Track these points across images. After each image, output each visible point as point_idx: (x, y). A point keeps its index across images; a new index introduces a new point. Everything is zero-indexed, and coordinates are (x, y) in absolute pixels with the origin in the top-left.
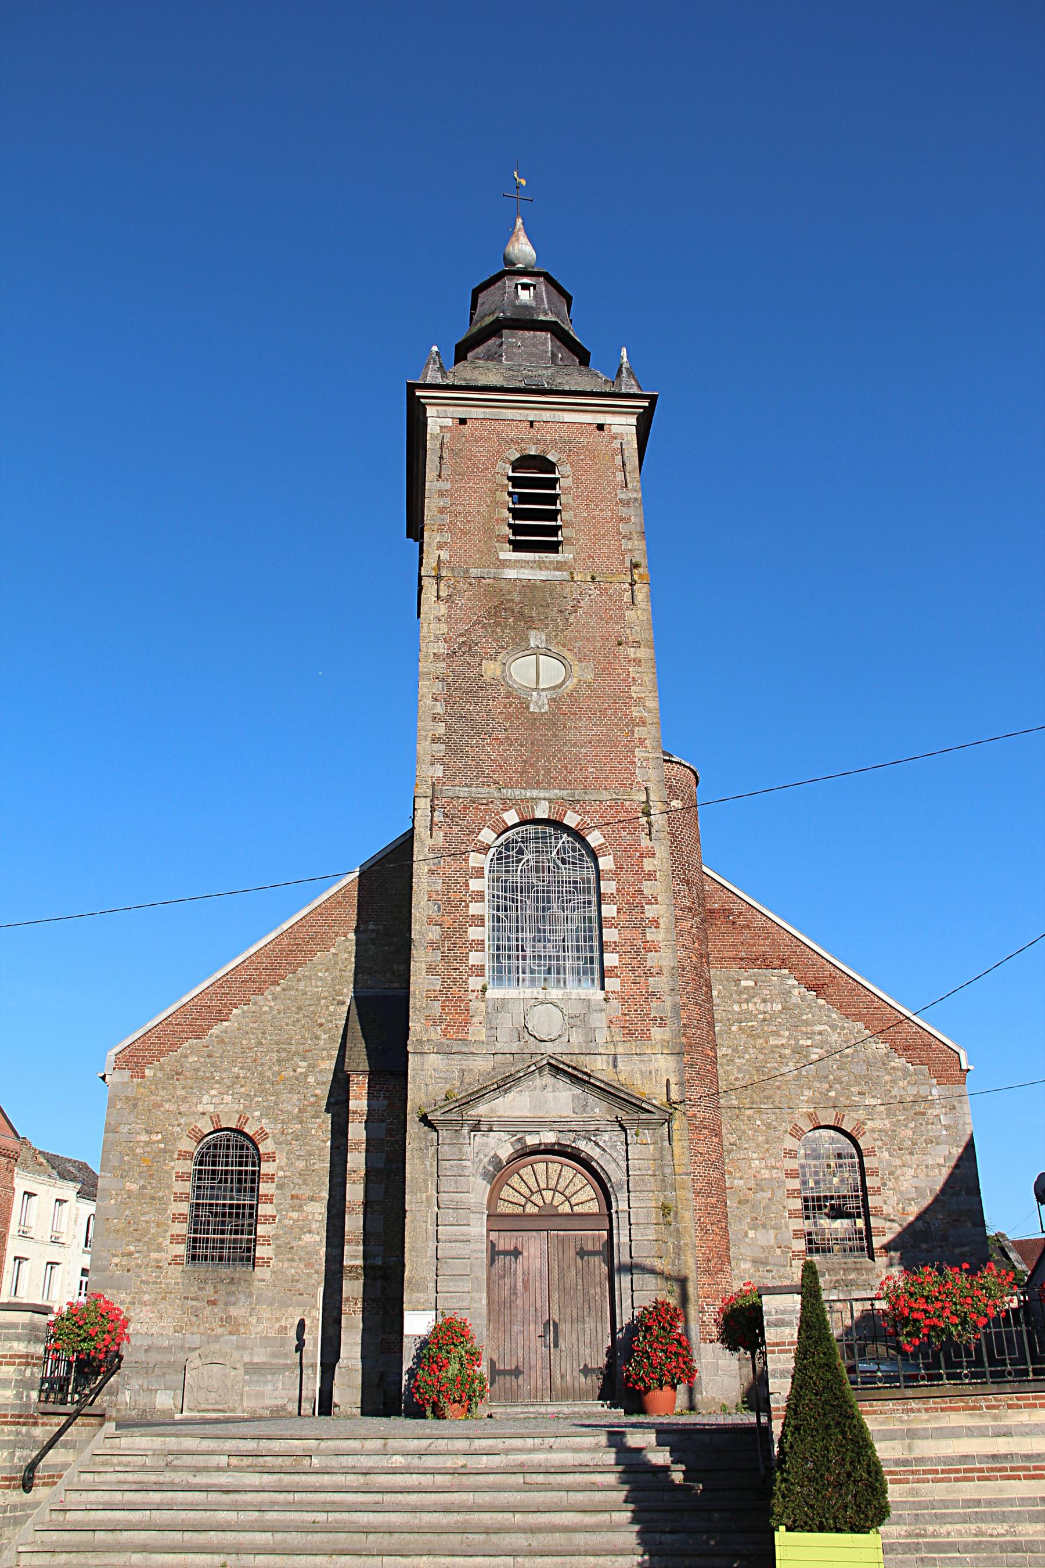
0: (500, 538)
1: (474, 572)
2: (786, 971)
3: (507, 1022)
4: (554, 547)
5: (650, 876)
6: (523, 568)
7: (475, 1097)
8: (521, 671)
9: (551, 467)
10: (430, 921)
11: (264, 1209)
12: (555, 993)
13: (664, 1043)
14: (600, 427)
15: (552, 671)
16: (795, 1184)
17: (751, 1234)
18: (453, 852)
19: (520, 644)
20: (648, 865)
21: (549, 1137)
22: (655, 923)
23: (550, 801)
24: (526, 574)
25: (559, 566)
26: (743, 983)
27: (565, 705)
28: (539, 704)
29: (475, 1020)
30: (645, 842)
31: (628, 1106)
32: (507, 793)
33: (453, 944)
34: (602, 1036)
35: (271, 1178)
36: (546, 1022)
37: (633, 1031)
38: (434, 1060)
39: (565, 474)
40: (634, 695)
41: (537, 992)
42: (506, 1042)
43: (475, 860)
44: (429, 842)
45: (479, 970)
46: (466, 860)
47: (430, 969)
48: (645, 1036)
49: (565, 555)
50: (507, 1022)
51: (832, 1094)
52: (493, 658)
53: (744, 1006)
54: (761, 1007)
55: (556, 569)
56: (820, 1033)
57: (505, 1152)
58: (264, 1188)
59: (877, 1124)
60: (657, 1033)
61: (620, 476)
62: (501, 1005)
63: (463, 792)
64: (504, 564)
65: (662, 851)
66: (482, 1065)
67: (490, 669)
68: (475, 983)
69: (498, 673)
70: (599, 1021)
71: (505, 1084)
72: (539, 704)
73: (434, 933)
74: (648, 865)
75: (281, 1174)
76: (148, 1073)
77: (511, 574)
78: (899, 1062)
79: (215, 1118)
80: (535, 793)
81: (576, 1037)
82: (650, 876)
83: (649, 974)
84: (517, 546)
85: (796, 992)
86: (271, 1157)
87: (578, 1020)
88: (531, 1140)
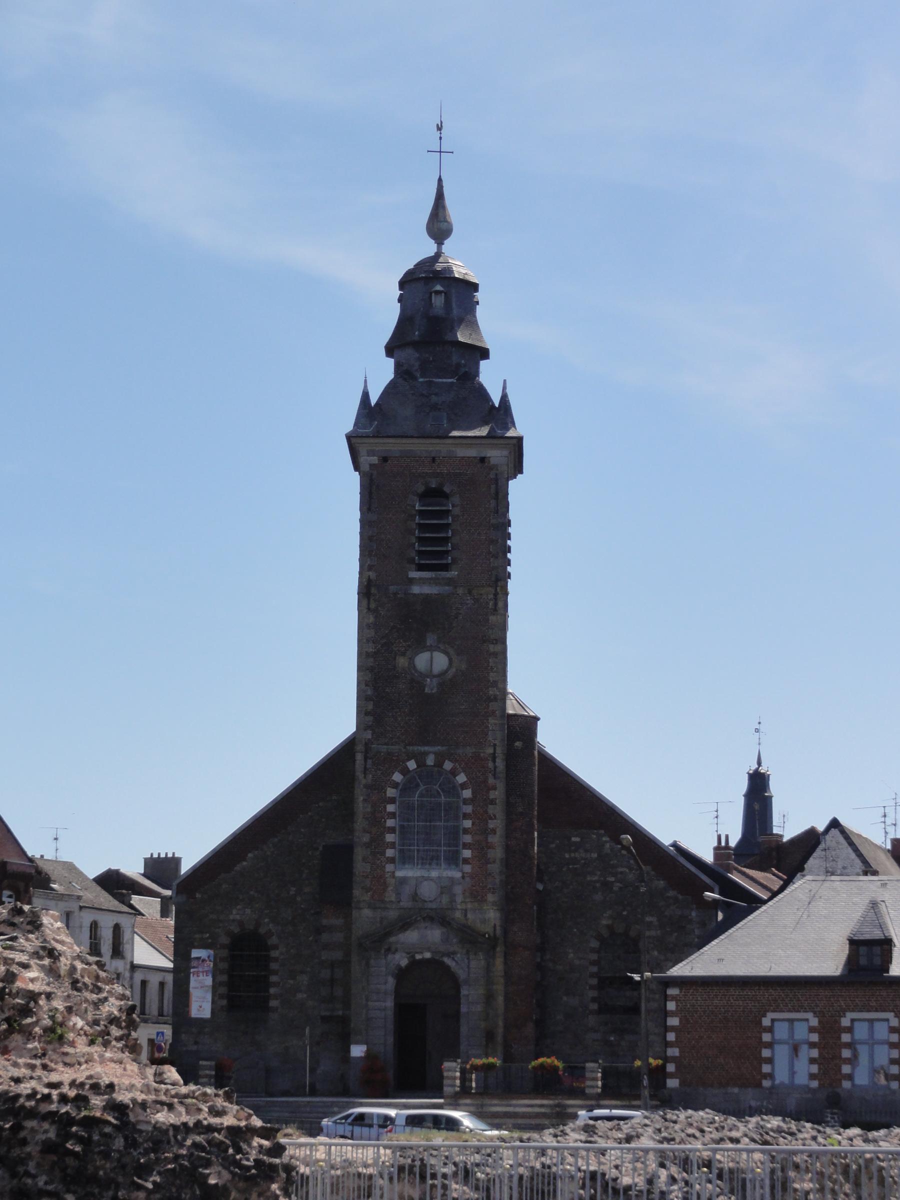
0: (411, 561)
1: (392, 588)
2: (603, 832)
3: (407, 890)
4: (445, 568)
5: (493, 802)
6: (423, 585)
7: (388, 934)
8: (422, 661)
9: (446, 496)
10: (365, 831)
11: (274, 979)
12: (434, 874)
13: (494, 903)
14: (483, 460)
15: (440, 661)
16: (594, 969)
17: (565, 998)
18: (377, 787)
19: (421, 646)
20: (493, 795)
21: (428, 955)
22: (494, 831)
23: (435, 753)
24: (427, 590)
25: (450, 582)
26: (573, 839)
27: (449, 684)
28: (431, 687)
29: (390, 888)
30: (491, 781)
31: (470, 938)
32: (411, 748)
33: (377, 845)
34: (459, 899)
35: (276, 960)
36: (428, 891)
37: (476, 896)
38: (367, 912)
39: (454, 505)
40: (491, 679)
41: (425, 873)
42: (406, 903)
43: (391, 792)
44: (364, 781)
45: (392, 860)
46: (385, 792)
47: (364, 859)
48: (483, 900)
49: (454, 573)
50: (407, 890)
51: (625, 913)
52: (403, 654)
53: (573, 855)
54: (583, 855)
55: (448, 584)
56: (621, 873)
57: (404, 962)
58: (274, 966)
59: (653, 933)
60: (491, 898)
61: (493, 502)
62: (403, 881)
63: (384, 749)
64: (411, 581)
65: (501, 786)
66: (393, 914)
67: (402, 662)
68: (389, 867)
69: (407, 664)
70: (458, 890)
71: (405, 924)
72: (431, 687)
73: (366, 838)
74: (493, 795)
75: (282, 957)
76: (198, 895)
77: (416, 590)
78: (671, 893)
79: (241, 924)
80: (426, 748)
81: (445, 900)
82: (493, 802)
83: (488, 862)
84: (421, 568)
85: (608, 845)
86: (276, 947)
87: (446, 888)
88: (418, 957)
